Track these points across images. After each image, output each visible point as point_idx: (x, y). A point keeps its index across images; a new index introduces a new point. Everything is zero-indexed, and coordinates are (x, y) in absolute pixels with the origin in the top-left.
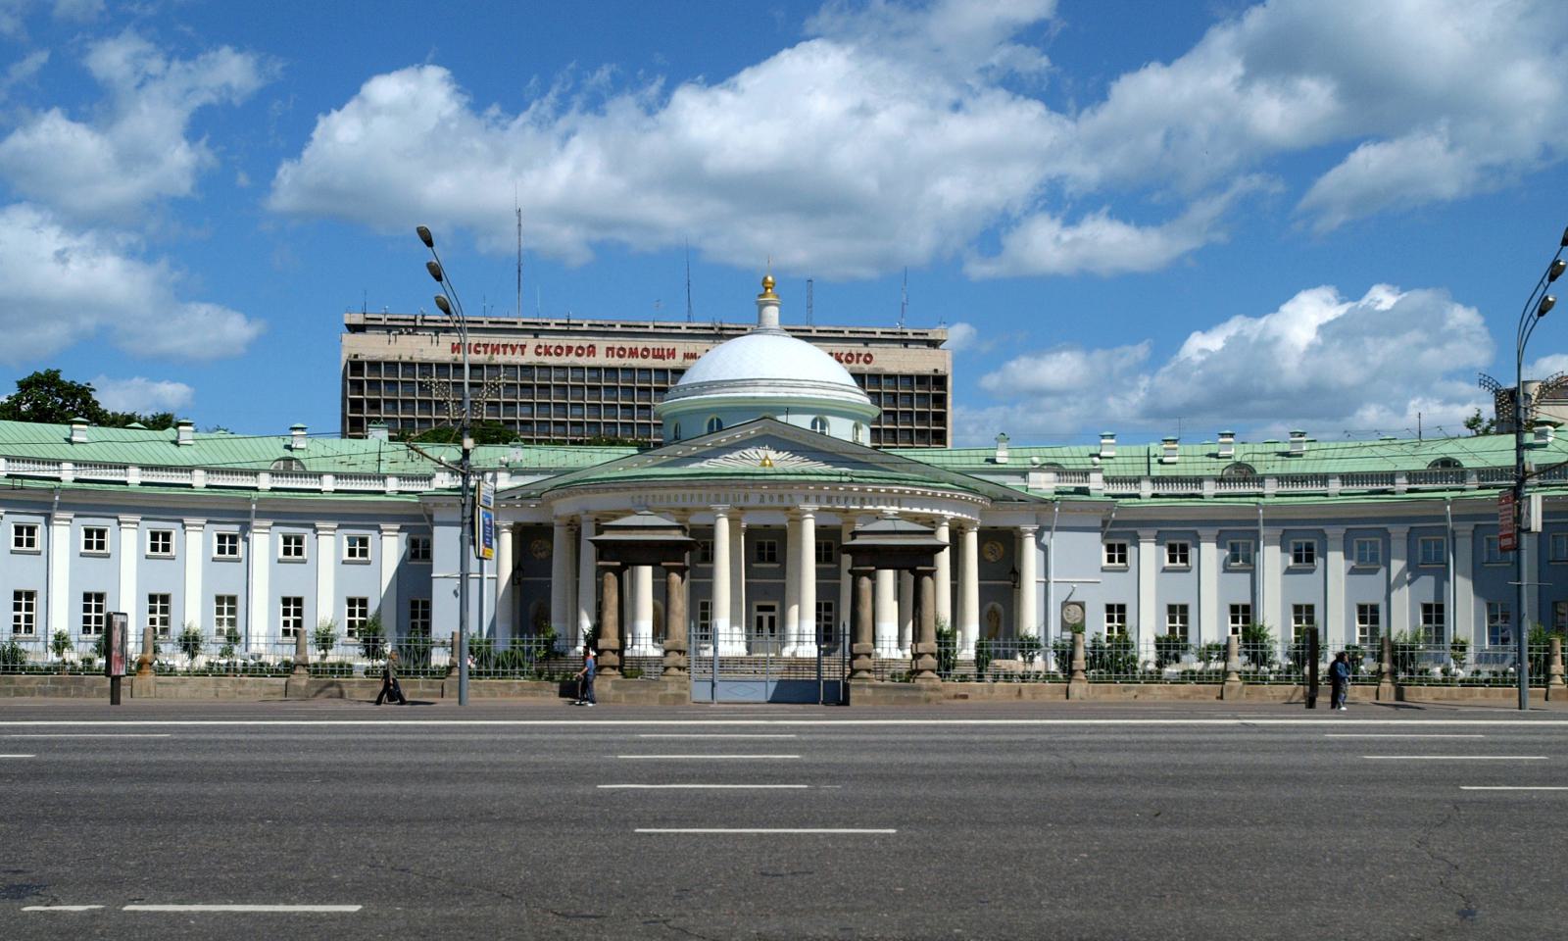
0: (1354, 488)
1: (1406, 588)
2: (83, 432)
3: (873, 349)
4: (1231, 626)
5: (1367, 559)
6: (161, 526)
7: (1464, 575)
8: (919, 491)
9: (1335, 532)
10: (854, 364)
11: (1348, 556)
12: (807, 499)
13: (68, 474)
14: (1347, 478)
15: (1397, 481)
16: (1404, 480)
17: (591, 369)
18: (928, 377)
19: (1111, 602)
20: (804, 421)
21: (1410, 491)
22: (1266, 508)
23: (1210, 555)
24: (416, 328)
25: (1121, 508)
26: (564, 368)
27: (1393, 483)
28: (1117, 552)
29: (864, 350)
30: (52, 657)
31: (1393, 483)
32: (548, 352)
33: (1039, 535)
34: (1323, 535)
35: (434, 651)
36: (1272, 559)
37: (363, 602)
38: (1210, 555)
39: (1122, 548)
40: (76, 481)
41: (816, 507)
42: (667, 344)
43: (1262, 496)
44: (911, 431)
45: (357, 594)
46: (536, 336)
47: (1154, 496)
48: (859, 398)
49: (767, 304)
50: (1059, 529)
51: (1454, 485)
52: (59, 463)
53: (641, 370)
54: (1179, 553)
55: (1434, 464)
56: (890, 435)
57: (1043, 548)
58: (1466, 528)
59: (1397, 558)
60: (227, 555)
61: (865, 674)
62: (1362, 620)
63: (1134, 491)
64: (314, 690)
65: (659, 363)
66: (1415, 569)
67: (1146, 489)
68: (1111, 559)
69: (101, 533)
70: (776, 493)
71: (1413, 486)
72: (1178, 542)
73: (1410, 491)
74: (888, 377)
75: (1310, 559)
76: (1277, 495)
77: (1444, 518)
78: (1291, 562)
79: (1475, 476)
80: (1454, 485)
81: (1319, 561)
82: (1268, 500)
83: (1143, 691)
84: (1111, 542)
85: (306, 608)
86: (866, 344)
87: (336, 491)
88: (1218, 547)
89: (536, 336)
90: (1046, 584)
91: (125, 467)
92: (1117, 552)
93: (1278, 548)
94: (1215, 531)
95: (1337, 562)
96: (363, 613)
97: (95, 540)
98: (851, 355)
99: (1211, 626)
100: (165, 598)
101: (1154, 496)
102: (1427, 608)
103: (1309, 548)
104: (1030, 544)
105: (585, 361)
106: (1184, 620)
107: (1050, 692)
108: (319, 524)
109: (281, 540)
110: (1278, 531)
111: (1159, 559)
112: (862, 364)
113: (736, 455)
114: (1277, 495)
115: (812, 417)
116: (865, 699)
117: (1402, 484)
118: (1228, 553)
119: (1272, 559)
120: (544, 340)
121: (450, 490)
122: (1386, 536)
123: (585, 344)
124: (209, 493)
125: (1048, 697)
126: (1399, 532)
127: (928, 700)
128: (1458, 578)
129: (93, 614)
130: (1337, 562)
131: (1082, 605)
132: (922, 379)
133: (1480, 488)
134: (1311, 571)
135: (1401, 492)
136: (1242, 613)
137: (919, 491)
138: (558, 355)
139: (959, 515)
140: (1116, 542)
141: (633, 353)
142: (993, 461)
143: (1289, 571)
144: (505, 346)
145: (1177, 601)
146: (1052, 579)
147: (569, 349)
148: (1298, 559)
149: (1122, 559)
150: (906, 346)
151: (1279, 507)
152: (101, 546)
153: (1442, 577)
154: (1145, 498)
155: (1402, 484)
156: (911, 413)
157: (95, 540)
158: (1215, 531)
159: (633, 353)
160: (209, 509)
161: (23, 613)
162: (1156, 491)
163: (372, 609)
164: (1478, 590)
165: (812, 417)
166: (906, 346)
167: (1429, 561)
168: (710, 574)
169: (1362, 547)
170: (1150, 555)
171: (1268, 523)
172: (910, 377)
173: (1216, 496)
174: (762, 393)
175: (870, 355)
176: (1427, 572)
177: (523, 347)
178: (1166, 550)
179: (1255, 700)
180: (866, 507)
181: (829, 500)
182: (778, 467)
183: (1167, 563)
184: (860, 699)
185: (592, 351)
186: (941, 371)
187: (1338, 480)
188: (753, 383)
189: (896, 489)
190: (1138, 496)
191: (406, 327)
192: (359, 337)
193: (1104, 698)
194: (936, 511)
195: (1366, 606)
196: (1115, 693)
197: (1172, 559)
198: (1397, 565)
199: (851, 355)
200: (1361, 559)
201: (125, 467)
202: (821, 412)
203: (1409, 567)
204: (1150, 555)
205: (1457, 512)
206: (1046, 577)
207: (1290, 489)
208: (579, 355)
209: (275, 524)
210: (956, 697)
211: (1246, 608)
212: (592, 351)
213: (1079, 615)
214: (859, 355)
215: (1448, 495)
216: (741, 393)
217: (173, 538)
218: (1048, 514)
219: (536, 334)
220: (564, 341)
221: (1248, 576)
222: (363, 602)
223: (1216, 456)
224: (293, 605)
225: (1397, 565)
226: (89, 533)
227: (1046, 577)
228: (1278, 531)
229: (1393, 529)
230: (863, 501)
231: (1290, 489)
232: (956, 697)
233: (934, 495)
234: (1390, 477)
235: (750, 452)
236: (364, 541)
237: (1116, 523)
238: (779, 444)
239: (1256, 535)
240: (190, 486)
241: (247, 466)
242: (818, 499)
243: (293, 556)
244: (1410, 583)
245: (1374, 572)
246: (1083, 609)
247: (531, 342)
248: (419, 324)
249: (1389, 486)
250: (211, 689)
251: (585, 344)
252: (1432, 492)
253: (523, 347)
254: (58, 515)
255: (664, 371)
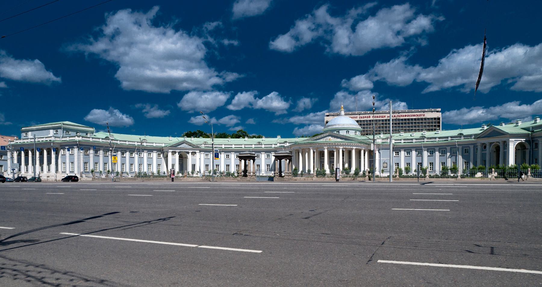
0: (441, 140)
1: (450, 159)
2: (246, 139)
3: (425, 113)
4: (206, 170)
5: (443, 152)
6: (228, 154)
7: (460, 155)
8: (347, 144)
9: (438, 148)
10: (421, 116)
11: (439, 153)
12: (325, 146)
13: (223, 146)
14: (439, 138)
15: (449, 138)
16: (450, 138)
17: (369, 120)
18: (436, 118)
19: (407, 162)
20: (343, 133)
21: (451, 140)
22: (423, 144)
23: (414, 153)
24: (338, 115)
25: (396, 145)
26: (403, 119)
27: (448, 139)
28: (397, 153)
29: (423, 113)
30: (208, 174)
31: (448, 139)
32: (361, 118)
33: (379, 151)
34: (435, 149)
35: (282, 173)
36: (426, 154)
37: (269, 165)
38: (414, 153)
39: (398, 152)
40: (225, 147)
41: (327, 147)
42: (384, 115)
43: (424, 142)
44: (429, 129)
45: (268, 164)
46: (360, 115)
47: (404, 142)
48: (359, 127)
49: (342, 111)
50: (382, 149)
51: (459, 138)
52: (232, 145)
53: (363, 121)
54: (408, 153)
55: (459, 134)
56: (429, 130)
57: (379, 153)
58: (460, 147)
59: (448, 152)
60: (228, 158)
61: (276, 176)
62: (442, 165)
63: (400, 142)
64: (206, 179)
65: (382, 119)
66: (451, 156)
67: (403, 141)
68: (396, 155)
69: (229, 155)
70: (320, 145)
71: (452, 139)
72: (408, 151)
73: (451, 140)
74: (428, 118)
75: (433, 154)
76: (427, 142)
77: (456, 145)
78: (429, 154)
79: (463, 137)
80: (459, 138)
81: (434, 154)
82: (424, 143)
83: (325, 179)
84: (396, 151)
85: (229, 166)
86: (424, 113)
87: (235, 147)
88: (416, 151)
89: (360, 115)
90: (380, 159)
91: (252, 145)
92: (397, 153)
93: (426, 151)
94: (415, 149)
95: (437, 154)
96: (269, 167)
97: (228, 156)
98: (420, 115)
99: (414, 167)
100: (259, 165)
101: (404, 142)
102: (454, 163)
103: (433, 151)
104: (377, 153)
105: (368, 119)
106: (433, 165)
107: (387, 180)
108: (262, 153)
109: (226, 155)
110: (426, 149)
111: (405, 154)
112: (423, 116)
113: (322, 139)
114: (427, 142)
115: (346, 131)
116: (276, 180)
117: (450, 139)
118: (417, 153)
119: (426, 154)
120: (361, 116)
121: (280, 146)
122: (446, 149)
123: (368, 116)
124: (265, 148)
125: (309, 180)
126: (448, 148)
127: (286, 181)
128: (459, 156)
129: (268, 168)
130: (437, 154)
131: (387, 163)
132: (435, 119)
133: (464, 139)
134: (433, 156)
135: (449, 140)
136: (420, 164)
137: (347, 144)
138: (363, 118)
139: (357, 148)
140: (397, 151)
141: (377, 117)
142: (380, 137)
143: (429, 156)
144: (353, 117)
145: (408, 162)
146: (381, 159)
147: (365, 117)
148: (430, 154)
149: (398, 154)
150: (432, 112)
151: (426, 144)
152: (229, 157)
153: (456, 156)
154: (402, 143)
155: (450, 139)
156: (433, 125)
157: (228, 156)
158: (415, 149)
159: (377, 117)
160: (225, 151)
161: (258, 168)
162: (404, 142)
163: (271, 166)
164: (463, 158)
165: (346, 131)
166: (432, 112)
167: (454, 154)
168: (324, 159)
169: (442, 151)
170: (403, 153)
171: (424, 147)
172: (433, 118)
173: (415, 142)
174: (337, 126)
175: (424, 115)
176: (454, 156)
177: (357, 117)
178: (406, 153)
179: (344, 180)
180: (336, 147)
181: (329, 146)
182: (332, 140)
183: (406, 155)
184: (276, 180)
185: (370, 117)
186: (439, 117)
187: (438, 138)
188: (335, 125)
189: (342, 144)
190: (401, 143)
191: (336, 115)
192: (328, 117)
193: (318, 180)
194: (351, 147)
195: (443, 163)
196: (321, 179)
197: (407, 154)
198: (448, 154)
199: (420, 115)
200: (442, 153)
201: (252, 145)
202: (348, 130)
203: (450, 155)
204: (403, 153)
205: (458, 144)
206: (380, 158)
207: (417, 141)
208: (408, 117)
209: (265, 153)
210: (295, 180)
211: (421, 163)
212: (370, 117)
213: (386, 165)
214: (422, 115)
215: (456, 141)
216: (334, 127)
217: (230, 156)
218: (381, 147)
219: (360, 115)
220: (364, 116)
221: (421, 157)
222: (269, 165)
223: (436, 133)
224: (207, 166)
225: (448, 154)
226: (227, 155)
227: (380, 158)
228: (426, 149)
229: (447, 148)
230: (336, 146)
231: (417, 141)
232: (295, 180)
233: (354, 144)
234: (447, 137)
235: (328, 137)
236: (269, 155)
237: (396, 148)
238: (332, 136)
239: (422, 149)
240: (232, 147)
241: (220, 144)
242: (327, 146)
243: (228, 158)
244: (450, 158)
245: (444, 156)
246: (387, 164)
247: (358, 116)
248: (338, 114)
249: (447, 139)
250: (193, 179)
251: (368, 116)
252: (456, 140)
253: (357, 117)
254: (222, 153)
255: (383, 120)
